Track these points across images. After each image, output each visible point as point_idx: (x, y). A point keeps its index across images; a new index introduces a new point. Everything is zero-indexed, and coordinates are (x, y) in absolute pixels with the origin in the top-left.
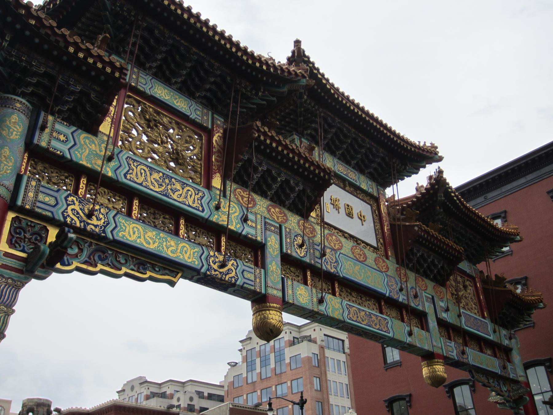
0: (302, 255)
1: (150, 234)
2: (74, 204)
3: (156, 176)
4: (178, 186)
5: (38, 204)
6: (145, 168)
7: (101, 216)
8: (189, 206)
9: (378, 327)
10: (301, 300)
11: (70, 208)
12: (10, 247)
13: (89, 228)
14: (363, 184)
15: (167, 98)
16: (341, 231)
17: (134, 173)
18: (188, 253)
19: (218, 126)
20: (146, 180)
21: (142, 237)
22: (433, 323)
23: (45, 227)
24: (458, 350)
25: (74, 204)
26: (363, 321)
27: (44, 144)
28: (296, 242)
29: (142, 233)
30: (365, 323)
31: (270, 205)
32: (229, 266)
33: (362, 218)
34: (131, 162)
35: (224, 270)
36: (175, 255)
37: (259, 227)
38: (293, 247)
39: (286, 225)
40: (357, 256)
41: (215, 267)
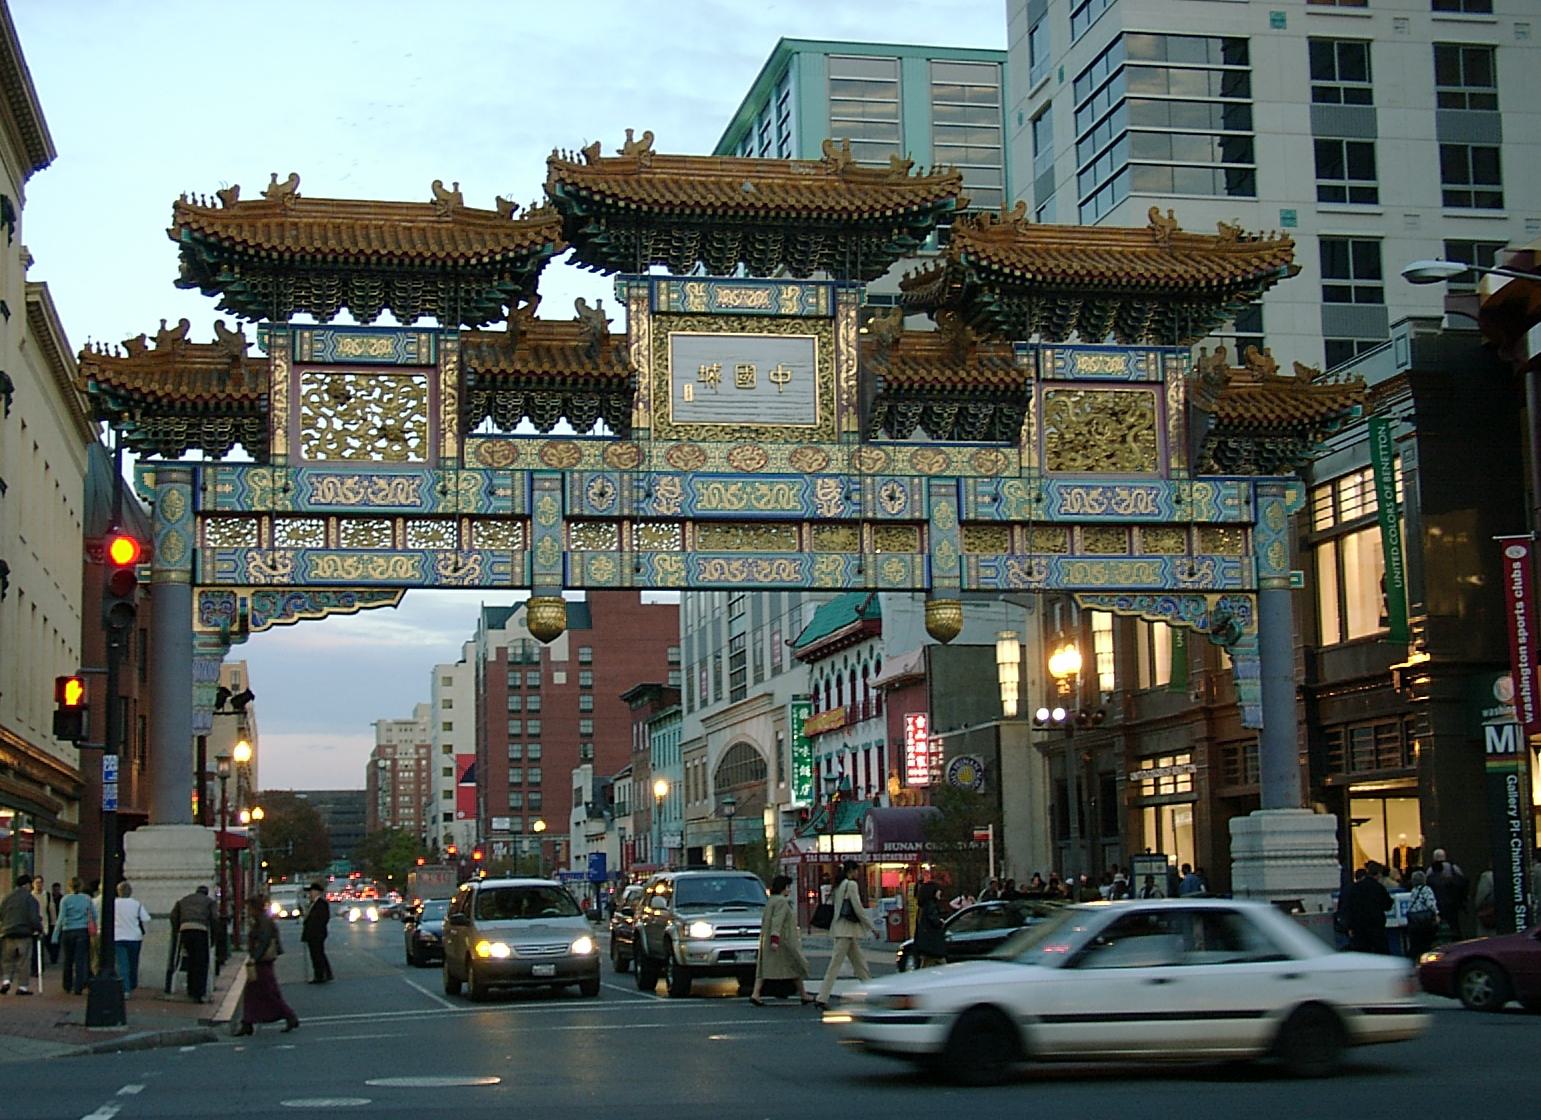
0: (605, 507)
1: (350, 561)
2: (255, 560)
3: (349, 482)
5: (218, 575)
6: (333, 480)
7: (287, 561)
9: (774, 575)
10: (598, 577)
11: (252, 565)
12: (204, 626)
13: (275, 581)
14: (789, 303)
15: (359, 352)
17: (320, 493)
18: (404, 568)
19: (447, 352)
21: (340, 568)
23: (232, 592)
25: (255, 560)
26: (735, 576)
27: (209, 507)
28: (590, 493)
29: (339, 563)
30: (740, 578)
31: (546, 445)
32: (471, 564)
34: (314, 480)
35: (461, 572)
36: (386, 576)
38: (585, 500)
39: (578, 467)
40: (743, 465)
41: (447, 573)
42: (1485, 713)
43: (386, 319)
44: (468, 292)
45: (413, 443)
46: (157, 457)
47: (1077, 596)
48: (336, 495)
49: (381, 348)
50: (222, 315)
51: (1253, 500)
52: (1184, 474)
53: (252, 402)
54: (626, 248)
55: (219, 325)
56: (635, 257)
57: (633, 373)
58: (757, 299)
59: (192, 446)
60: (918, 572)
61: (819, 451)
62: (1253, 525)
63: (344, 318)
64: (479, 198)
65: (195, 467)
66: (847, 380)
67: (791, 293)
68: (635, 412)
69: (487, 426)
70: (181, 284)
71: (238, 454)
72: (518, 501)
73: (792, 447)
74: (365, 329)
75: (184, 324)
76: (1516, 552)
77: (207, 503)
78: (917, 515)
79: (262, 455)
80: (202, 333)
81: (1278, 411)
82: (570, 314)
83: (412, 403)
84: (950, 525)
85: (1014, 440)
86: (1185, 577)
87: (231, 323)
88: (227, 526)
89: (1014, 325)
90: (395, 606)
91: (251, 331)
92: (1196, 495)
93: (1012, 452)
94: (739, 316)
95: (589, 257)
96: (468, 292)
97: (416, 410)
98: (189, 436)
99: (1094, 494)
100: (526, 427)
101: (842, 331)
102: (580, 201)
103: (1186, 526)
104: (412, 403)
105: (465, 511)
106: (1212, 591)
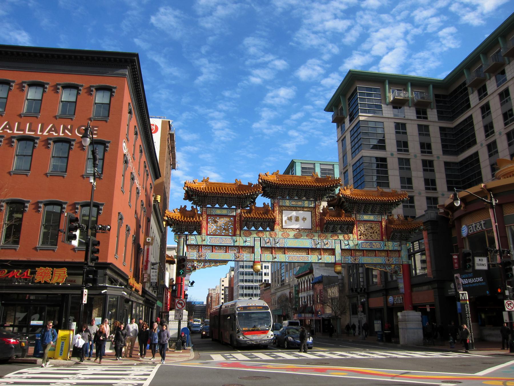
3: (217, 239)
4: (224, 239)
8: (228, 244)
16: (291, 229)
20: (215, 241)
22: (338, 251)
24: (353, 259)
27: (189, 243)
30: (296, 260)
33: (304, 219)
37: (252, 241)
42: (449, 291)
43: (226, 206)
44: (242, 201)
45: (230, 231)
46: (179, 233)
47: (365, 265)
48: (215, 241)
49: (224, 212)
50: (193, 205)
51: (400, 245)
52: (386, 240)
53: (199, 222)
54: (274, 193)
55: (192, 207)
56: (275, 195)
57: (275, 218)
58: (300, 203)
59: (186, 231)
60: (333, 259)
61: (312, 234)
62: (401, 251)
63: (217, 206)
64: (245, 183)
65: (186, 235)
66: (318, 220)
67: (306, 202)
68: (275, 226)
69: (245, 228)
70: (185, 199)
71: (195, 233)
72: (251, 243)
73: (307, 233)
74: (221, 208)
75: (185, 206)
76: (455, 257)
77: (188, 243)
78: (332, 248)
79: (200, 233)
80: (189, 208)
81: (405, 227)
82: (262, 206)
83: (230, 223)
84: (339, 250)
85: (351, 232)
86: (387, 261)
87: (195, 207)
88: (192, 247)
89: (351, 209)
90: (226, 265)
91: (199, 208)
92: (389, 244)
93: (351, 235)
94: (296, 207)
95: (265, 195)
96: (242, 201)
97: (231, 225)
98: (186, 229)
99: (368, 244)
100: (253, 228)
101: (317, 210)
102: (265, 183)
103: (387, 251)
104: (230, 223)
105: (241, 245)
106: (393, 264)
